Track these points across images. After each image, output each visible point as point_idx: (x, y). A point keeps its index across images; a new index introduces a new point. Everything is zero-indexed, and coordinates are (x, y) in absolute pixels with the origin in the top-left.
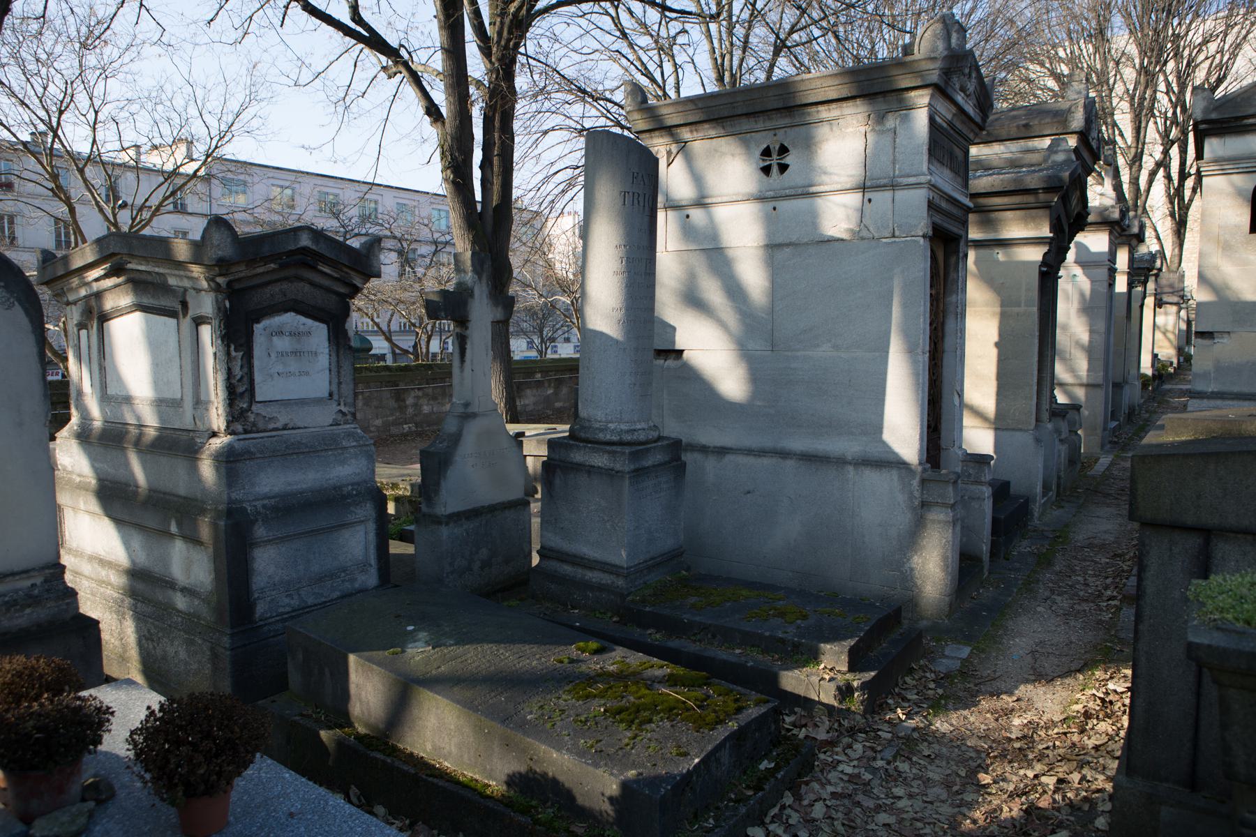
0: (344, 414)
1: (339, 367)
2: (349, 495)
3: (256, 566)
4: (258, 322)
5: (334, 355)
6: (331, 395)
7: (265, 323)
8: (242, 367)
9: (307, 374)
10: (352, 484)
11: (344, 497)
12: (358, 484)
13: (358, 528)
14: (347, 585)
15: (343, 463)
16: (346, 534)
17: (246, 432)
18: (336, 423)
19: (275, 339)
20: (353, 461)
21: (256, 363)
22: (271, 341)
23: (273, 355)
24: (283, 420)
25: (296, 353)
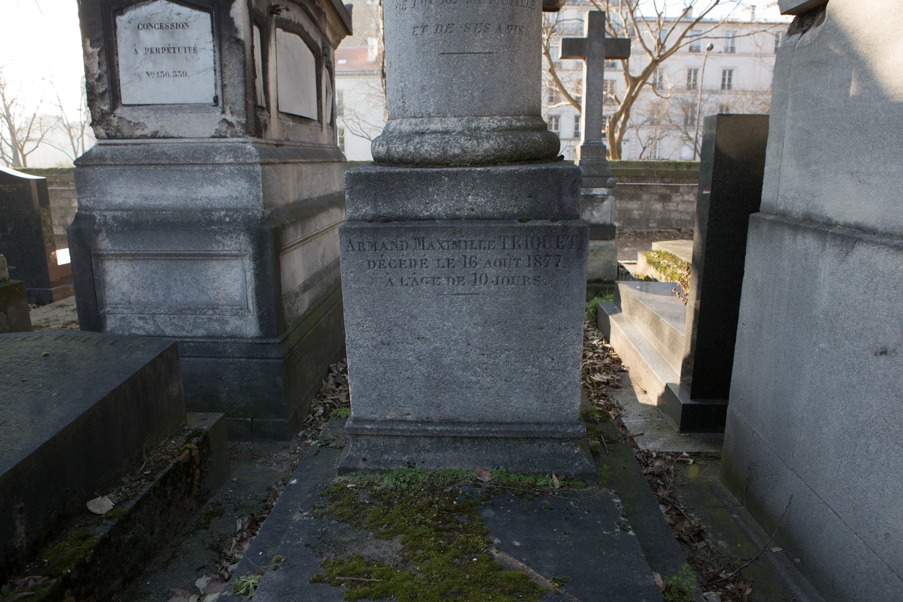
0: (230, 124)
1: (222, 66)
2: (220, 221)
3: (108, 279)
4: (121, 13)
5: (217, 50)
6: (216, 99)
7: (131, 14)
8: (99, 64)
9: (185, 74)
10: (228, 210)
11: (211, 222)
12: (236, 210)
13: (233, 263)
14: (216, 325)
15: (214, 182)
16: (217, 267)
17: (109, 137)
18: (219, 135)
19: (142, 33)
20: (229, 182)
21: (122, 61)
22: (138, 35)
23: (141, 52)
24: (151, 126)
25: (169, 49)
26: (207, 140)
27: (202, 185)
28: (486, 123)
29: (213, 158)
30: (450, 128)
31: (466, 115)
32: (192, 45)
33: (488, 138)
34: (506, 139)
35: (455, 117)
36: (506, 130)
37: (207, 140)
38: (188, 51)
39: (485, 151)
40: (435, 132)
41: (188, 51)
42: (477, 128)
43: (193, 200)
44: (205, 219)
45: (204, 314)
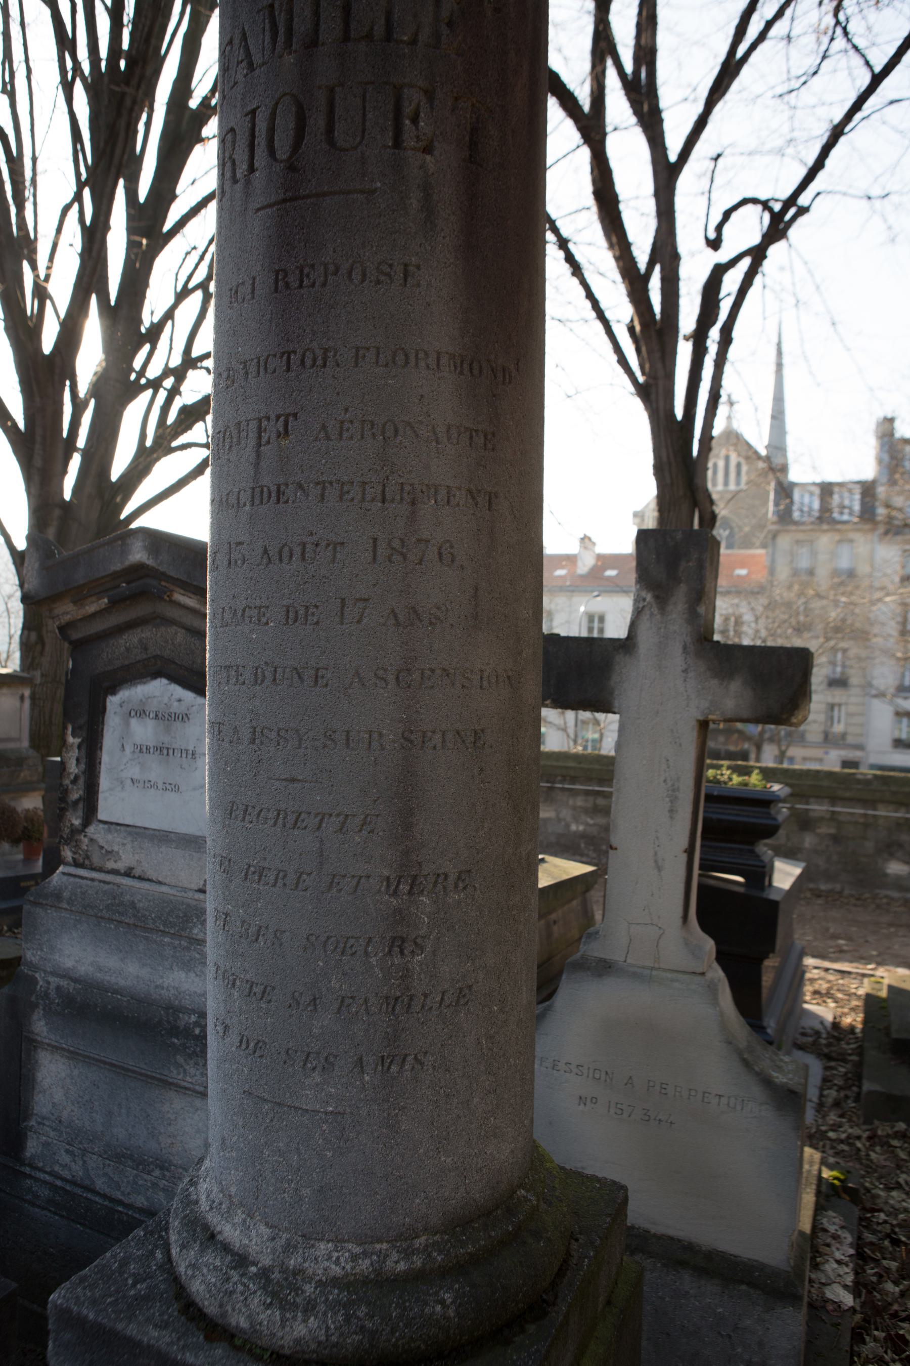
3: (39, 1076)
4: (114, 693)
7: (124, 694)
8: (78, 760)
9: (176, 788)
11: (174, 1031)
17: (76, 864)
19: (134, 722)
21: (105, 758)
22: (127, 724)
23: (129, 749)
24: (126, 860)
25: (163, 750)
26: (190, 894)
27: (171, 968)
28: (328, 1260)
29: (191, 929)
30: (253, 1250)
31: (287, 1229)
32: (191, 748)
33: (309, 1308)
34: (348, 1319)
35: (267, 1224)
36: (365, 1281)
37: (190, 894)
38: (184, 755)
39: (298, 1341)
40: (226, 1248)
41: (184, 755)
42: (299, 1272)
43: (157, 987)
44: (169, 1022)
45: (149, 1173)
